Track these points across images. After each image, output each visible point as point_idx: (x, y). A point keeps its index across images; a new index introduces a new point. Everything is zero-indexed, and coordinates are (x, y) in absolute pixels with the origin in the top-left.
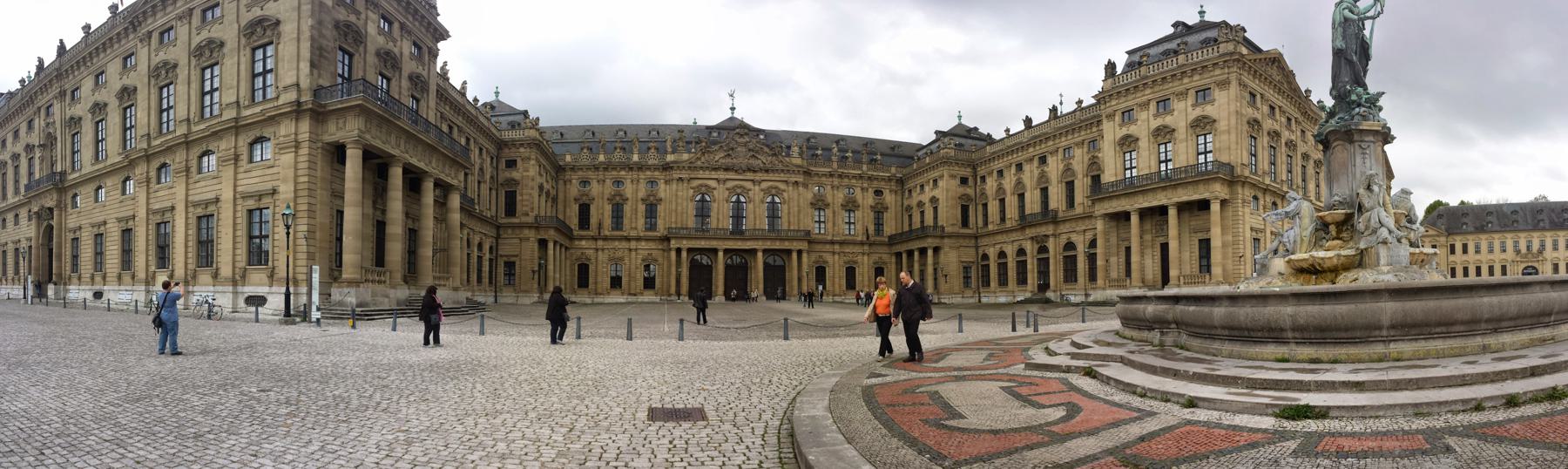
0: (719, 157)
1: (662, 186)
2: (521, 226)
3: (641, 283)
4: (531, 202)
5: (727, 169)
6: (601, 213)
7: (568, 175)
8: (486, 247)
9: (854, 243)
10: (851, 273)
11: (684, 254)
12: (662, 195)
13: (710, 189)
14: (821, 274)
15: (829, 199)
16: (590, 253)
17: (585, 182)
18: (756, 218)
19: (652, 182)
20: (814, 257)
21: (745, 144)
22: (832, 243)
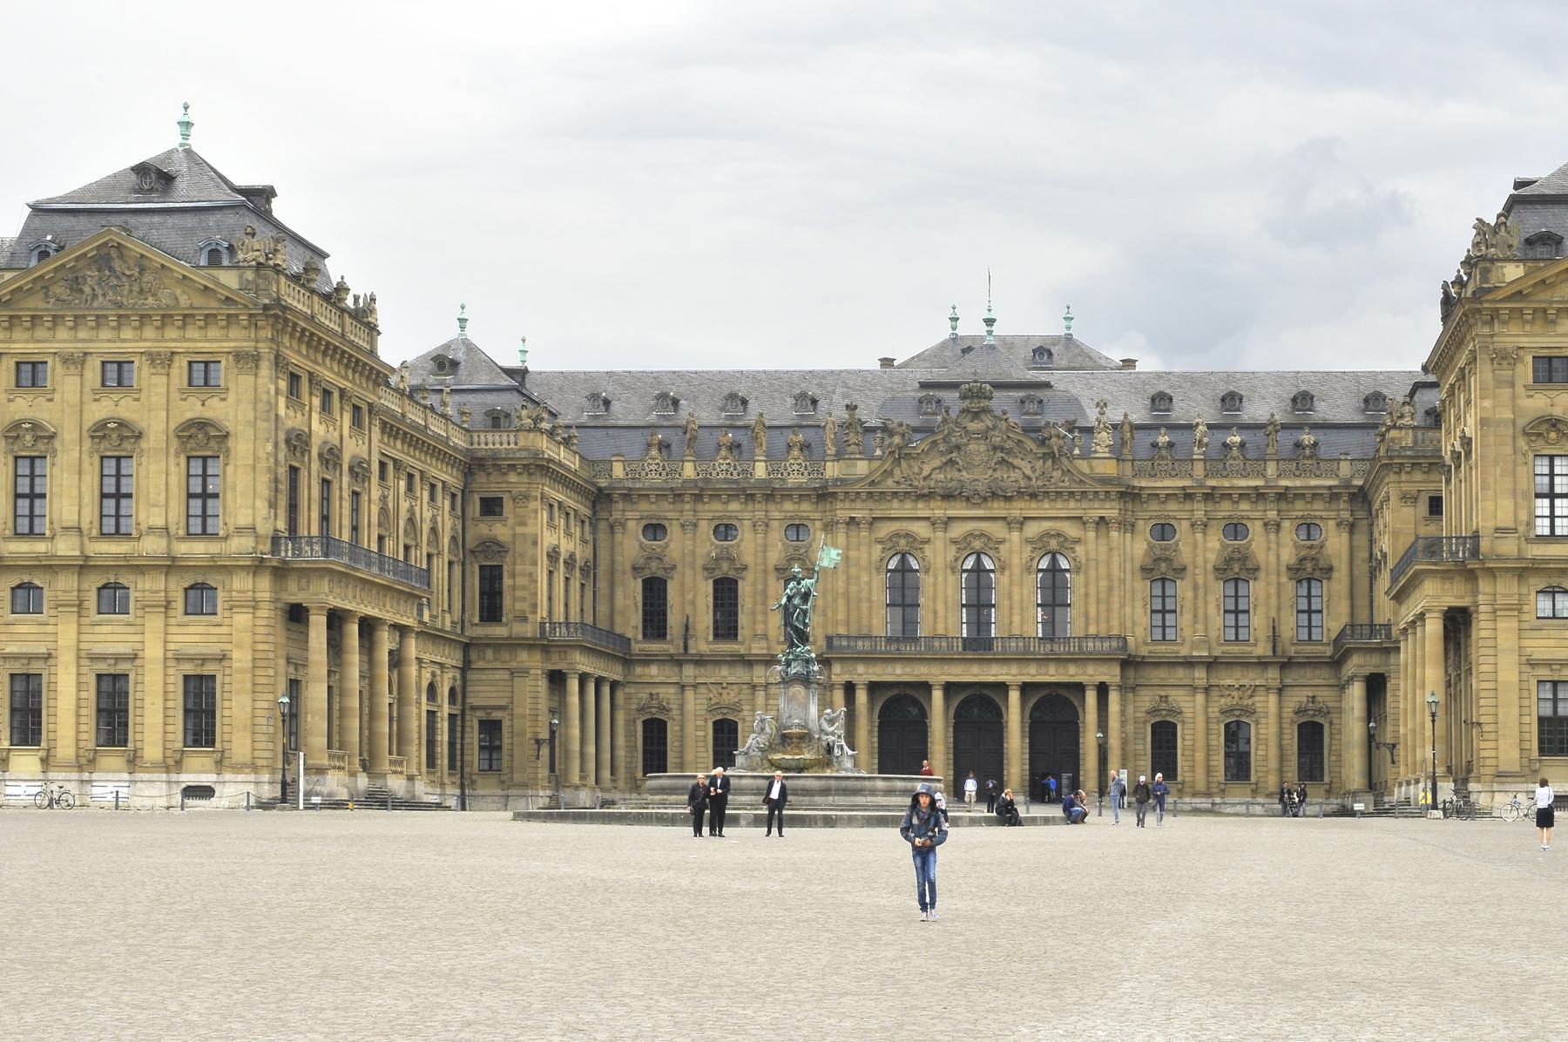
2: (513, 644)
4: (542, 594)
5: (948, 497)
8: (444, 691)
9: (1244, 663)
14: (1164, 738)
15: (1185, 554)
18: (1018, 611)
20: (1146, 699)
21: (985, 435)
22: (1189, 663)
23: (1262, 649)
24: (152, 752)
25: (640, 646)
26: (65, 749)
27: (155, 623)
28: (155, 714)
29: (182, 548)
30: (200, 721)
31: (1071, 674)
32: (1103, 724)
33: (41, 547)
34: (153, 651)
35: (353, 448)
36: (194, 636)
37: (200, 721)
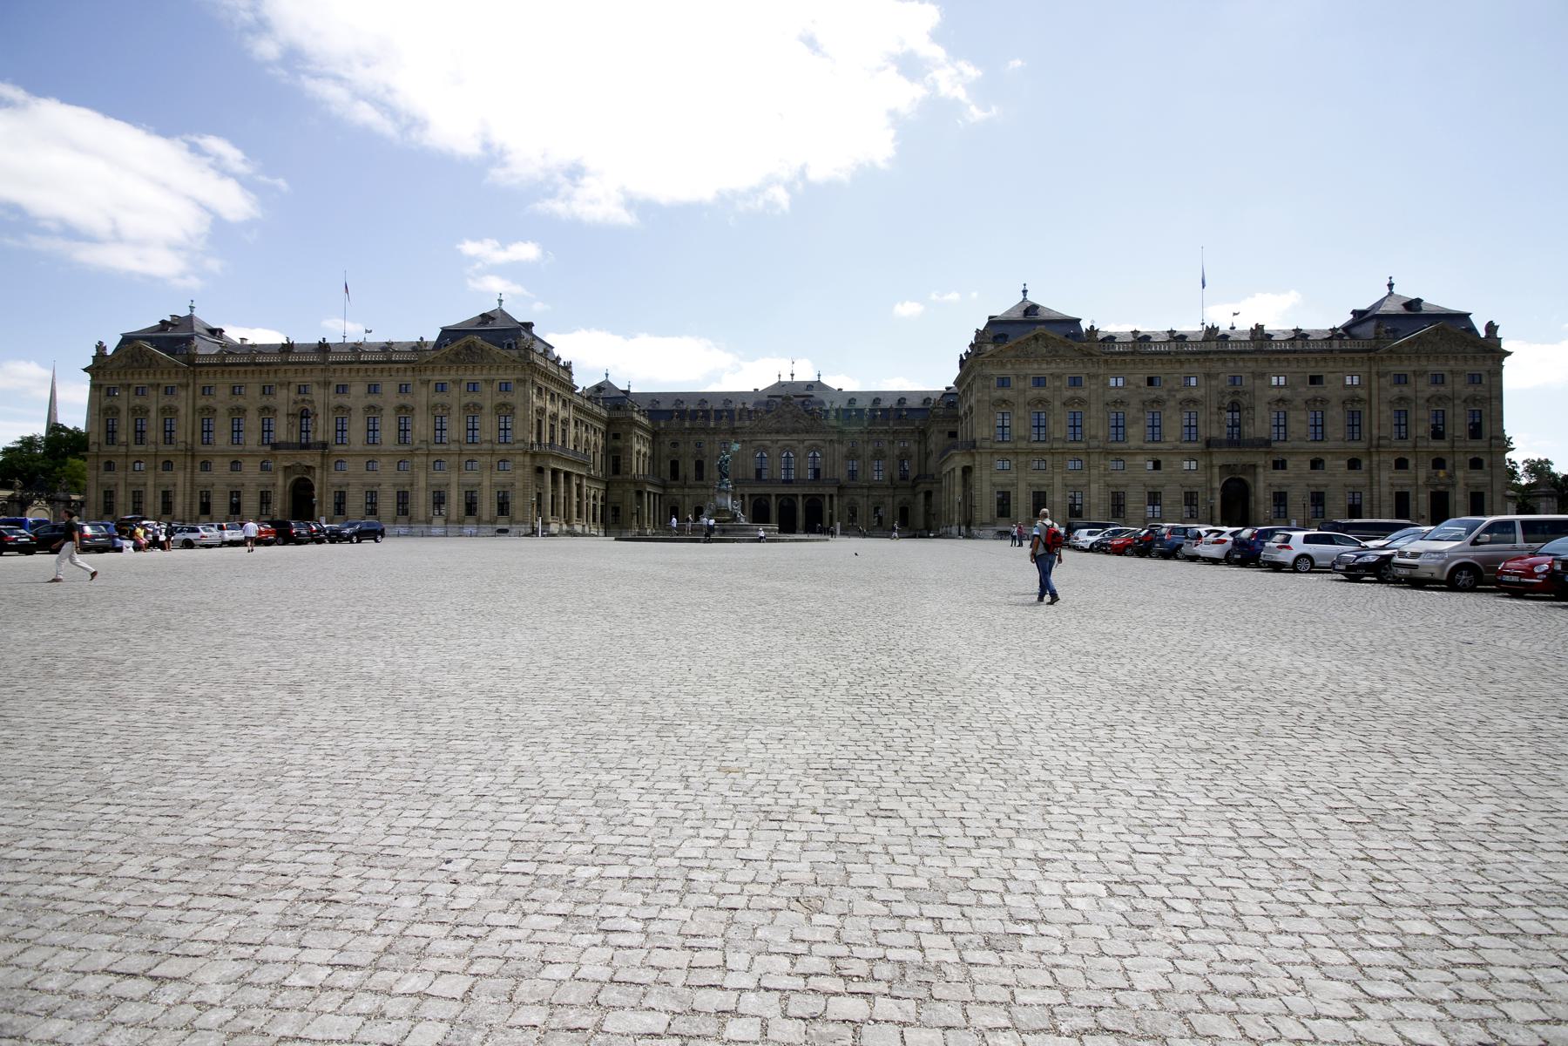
5: (778, 432)
13: (765, 449)
20: (846, 500)
24: (486, 517)
25: (670, 482)
26: (453, 517)
31: (821, 491)
32: (831, 507)
34: (486, 483)
35: (562, 414)
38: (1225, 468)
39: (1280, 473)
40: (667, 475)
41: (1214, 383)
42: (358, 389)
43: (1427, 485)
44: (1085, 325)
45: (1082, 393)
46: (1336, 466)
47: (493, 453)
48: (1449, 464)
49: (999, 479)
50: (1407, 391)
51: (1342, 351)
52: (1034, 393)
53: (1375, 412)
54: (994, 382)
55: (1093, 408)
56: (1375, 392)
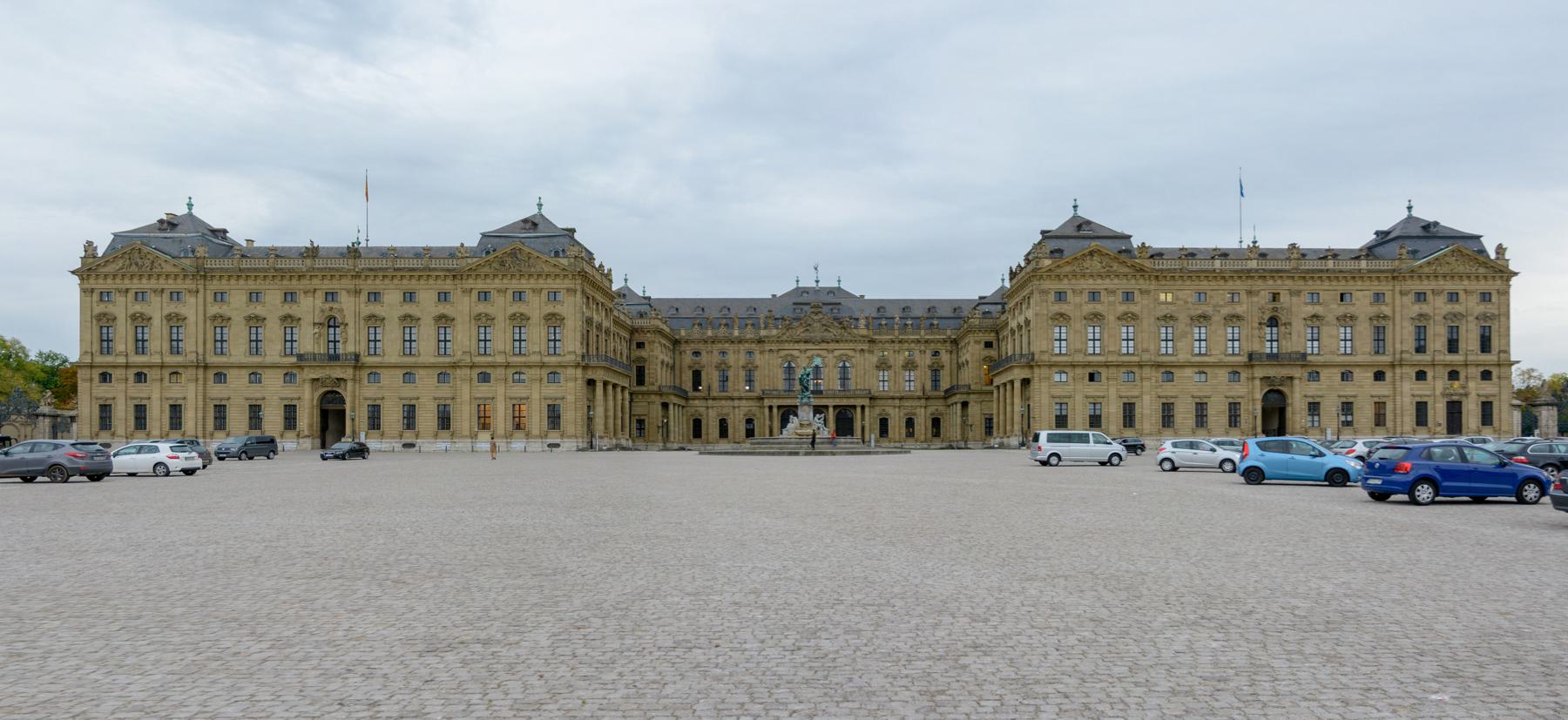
0: (799, 332)
1: (757, 356)
3: (743, 433)
6: (711, 377)
7: (683, 347)
10: (910, 423)
11: (775, 410)
12: (758, 362)
15: (891, 362)
16: (702, 410)
17: (697, 353)
19: (750, 353)
20: (877, 411)
23: (919, 393)
27: (536, 386)
28: (536, 418)
29: (546, 359)
30: (554, 418)
31: (852, 402)
32: (863, 419)
33: (489, 359)
34: (536, 396)
35: (606, 324)
36: (552, 390)
37: (554, 418)
38: (1265, 379)
39: (1314, 385)
40: (688, 386)
41: (1255, 299)
42: (392, 297)
43: (1443, 395)
44: (1136, 243)
45: (1134, 309)
46: (1364, 377)
47: (542, 366)
48: (1462, 376)
49: (1057, 391)
50: (1425, 309)
51: (1369, 271)
52: (1089, 308)
53: (1398, 328)
54: (1052, 297)
55: (1145, 323)
56: (1398, 309)
